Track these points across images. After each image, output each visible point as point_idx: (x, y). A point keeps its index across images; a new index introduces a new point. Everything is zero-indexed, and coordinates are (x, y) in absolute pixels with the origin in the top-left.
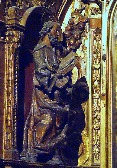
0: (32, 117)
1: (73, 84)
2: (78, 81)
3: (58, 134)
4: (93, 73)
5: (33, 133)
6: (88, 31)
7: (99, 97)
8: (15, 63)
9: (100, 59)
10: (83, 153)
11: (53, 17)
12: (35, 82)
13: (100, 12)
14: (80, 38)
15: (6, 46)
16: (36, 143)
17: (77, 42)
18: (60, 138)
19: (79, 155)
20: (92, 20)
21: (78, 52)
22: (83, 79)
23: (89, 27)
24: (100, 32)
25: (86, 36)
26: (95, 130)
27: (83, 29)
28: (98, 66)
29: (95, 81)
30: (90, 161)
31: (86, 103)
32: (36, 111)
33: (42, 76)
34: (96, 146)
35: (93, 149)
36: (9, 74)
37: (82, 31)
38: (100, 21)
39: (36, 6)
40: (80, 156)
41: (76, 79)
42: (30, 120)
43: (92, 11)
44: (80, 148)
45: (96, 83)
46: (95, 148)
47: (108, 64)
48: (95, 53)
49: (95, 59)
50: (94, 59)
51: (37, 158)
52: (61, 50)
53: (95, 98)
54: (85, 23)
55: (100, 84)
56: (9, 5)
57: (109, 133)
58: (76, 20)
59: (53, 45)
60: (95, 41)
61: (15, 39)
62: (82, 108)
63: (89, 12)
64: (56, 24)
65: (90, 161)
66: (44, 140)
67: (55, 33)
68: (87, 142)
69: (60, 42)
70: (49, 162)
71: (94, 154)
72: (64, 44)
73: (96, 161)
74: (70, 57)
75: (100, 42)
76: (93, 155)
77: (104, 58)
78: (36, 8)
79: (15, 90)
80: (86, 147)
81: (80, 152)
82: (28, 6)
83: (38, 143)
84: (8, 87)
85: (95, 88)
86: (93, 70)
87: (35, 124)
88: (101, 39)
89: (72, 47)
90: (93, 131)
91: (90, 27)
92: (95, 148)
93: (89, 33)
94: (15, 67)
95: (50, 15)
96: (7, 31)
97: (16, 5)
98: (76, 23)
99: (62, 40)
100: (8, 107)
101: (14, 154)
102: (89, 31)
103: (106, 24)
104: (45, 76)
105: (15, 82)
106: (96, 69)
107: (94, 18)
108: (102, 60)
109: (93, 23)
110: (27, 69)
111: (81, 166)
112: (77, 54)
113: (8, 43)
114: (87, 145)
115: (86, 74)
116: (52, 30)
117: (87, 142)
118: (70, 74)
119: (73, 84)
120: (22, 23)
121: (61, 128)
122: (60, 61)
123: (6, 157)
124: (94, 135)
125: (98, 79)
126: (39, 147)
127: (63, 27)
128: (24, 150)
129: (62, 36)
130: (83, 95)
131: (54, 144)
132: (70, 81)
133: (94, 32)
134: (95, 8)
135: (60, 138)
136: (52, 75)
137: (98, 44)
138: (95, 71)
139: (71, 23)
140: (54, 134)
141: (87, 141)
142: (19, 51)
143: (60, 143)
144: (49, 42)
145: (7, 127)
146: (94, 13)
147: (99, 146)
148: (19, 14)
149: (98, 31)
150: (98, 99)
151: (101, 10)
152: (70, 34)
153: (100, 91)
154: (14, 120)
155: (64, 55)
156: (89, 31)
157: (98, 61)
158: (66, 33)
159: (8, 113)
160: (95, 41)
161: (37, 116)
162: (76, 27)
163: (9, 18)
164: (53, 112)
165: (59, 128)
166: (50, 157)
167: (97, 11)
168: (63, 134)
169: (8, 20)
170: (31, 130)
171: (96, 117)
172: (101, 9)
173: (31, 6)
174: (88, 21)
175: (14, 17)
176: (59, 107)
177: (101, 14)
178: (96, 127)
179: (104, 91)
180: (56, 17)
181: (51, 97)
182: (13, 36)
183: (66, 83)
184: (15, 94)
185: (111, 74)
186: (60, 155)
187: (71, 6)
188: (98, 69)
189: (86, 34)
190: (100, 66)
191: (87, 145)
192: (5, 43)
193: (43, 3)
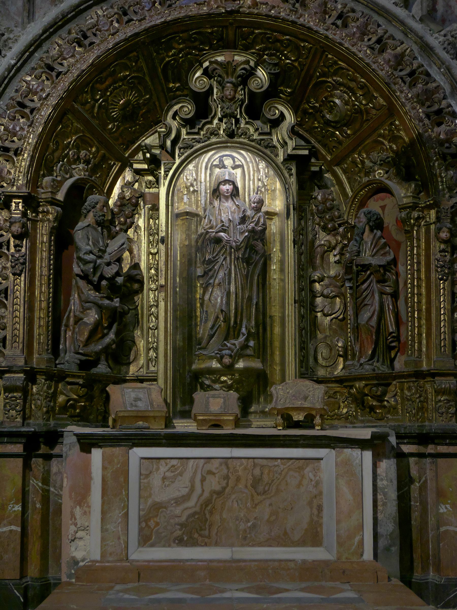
0: (72, 314)
1: (124, 272)
2: (130, 268)
4: (148, 259)
5: (72, 334)
6: (142, 208)
7: (157, 289)
8: (50, 246)
9: (158, 242)
10: (135, 359)
11: (98, 190)
12: (76, 270)
13: (157, 186)
14: (132, 216)
15: (39, 225)
16: (78, 347)
17: (128, 220)
18: (107, 340)
19: (131, 360)
20: (148, 195)
21: (130, 232)
22: (136, 266)
23: (144, 203)
24: (158, 210)
25: (140, 214)
26: (152, 329)
27: (137, 205)
28: (156, 250)
29: (151, 269)
30: (145, 368)
31: (140, 296)
32: (78, 306)
33: (86, 262)
34: (152, 350)
35: (148, 353)
36: (42, 259)
37: (134, 208)
38: (157, 196)
39: (77, 177)
40: (133, 361)
41: (128, 266)
42: (68, 317)
43: (146, 184)
44: (133, 353)
45: (153, 271)
46: (151, 353)
47: (167, 249)
48: (151, 235)
49: (151, 242)
50: (149, 242)
51: (79, 365)
52: (109, 231)
53: (152, 290)
54: (139, 198)
55: (158, 273)
56: (44, 176)
57: (169, 334)
58: (128, 194)
59: (99, 224)
60: (151, 220)
61: (50, 217)
62: (135, 303)
63: (144, 185)
64: (102, 198)
65: (145, 368)
66: (87, 342)
67: (102, 210)
68: (141, 344)
69: (107, 220)
70: (94, 371)
71: (150, 359)
72: (112, 222)
73: (152, 369)
74: (120, 240)
75: (157, 221)
76: (149, 360)
77: (163, 241)
78: (78, 179)
79: (49, 279)
80: (140, 351)
81: (132, 358)
82: (68, 176)
83: (79, 346)
84: (41, 275)
85: (151, 278)
86: (149, 256)
87: (76, 323)
88: (158, 218)
89: (122, 227)
90: (149, 331)
91: (145, 204)
92: (151, 353)
93: (144, 210)
94: (50, 250)
95: (95, 188)
96: (39, 206)
97: (52, 175)
98: (127, 198)
99: (110, 218)
100: (41, 301)
101: (49, 361)
102: (144, 207)
103: (165, 200)
104: (90, 262)
105: (50, 270)
106: (152, 254)
107: (150, 193)
108: (160, 244)
109: (148, 198)
110: (66, 253)
111: (133, 374)
112: (128, 235)
113: (42, 221)
114: (142, 349)
115: (140, 260)
116: (98, 206)
117: (141, 344)
118: (119, 260)
119: (124, 272)
120: (60, 196)
121: (110, 327)
122: (108, 244)
123: (37, 365)
124: (150, 336)
125: (155, 266)
126: (81, 351)
127: (111, 202)
128: (62, 355)
129: (110, 213)
130: (136, 286)
131: (100, 347)
132: (121, 268)
133: (150, 209)
134: (150, 181)
135: (107, 340)
136: (99, 261)
137: (155, 223)
138: (151, 256)
139: (121, 197)
140: (100, 335)
141: (141, 344)
142: (55, 231)
143: (108, 346)
144: (94, 220)
145: (40, 326)
146: (149, 186)
147: (156, 349)
148: (57, 186)
149: (155, 208)
150: (155, 291)
151: (158, 184)
152: (121, 211)
153: (157, 281)
154: (49, 317)
155: (112, 237)
156: (144, 207)
157: (155, 244)
158: (115, 210)
159: (40, 309)
160: (151, 220)
161: (77, 313)
162: (127, 202)
163: (43, 191)
164: (100, 307)
165: (106, 328)
166: (95, 363)
167: (154, 184)
168: (112, 336)
169: (43, 193)
170: (70, 330)
171: (152, 314)
172: (158, 181)
173: (71, 177)
174: (142, 195)
175: (50, 190)
176: (106, 302)
177: (158, 188)
178: (153, 326)
179: (162, 282)
180: (102, 189)
181: (97, 288)
182: (48, 212)
183: (115, 271)
184: (49, 284)
185: (171, 261)
186: (107, 361)
187: (121, 177)
188: (155, 254)
189: (140, 212)
190: (158, 251)
191: (142, 349)
192: (38, 221)
193: (87, 173)
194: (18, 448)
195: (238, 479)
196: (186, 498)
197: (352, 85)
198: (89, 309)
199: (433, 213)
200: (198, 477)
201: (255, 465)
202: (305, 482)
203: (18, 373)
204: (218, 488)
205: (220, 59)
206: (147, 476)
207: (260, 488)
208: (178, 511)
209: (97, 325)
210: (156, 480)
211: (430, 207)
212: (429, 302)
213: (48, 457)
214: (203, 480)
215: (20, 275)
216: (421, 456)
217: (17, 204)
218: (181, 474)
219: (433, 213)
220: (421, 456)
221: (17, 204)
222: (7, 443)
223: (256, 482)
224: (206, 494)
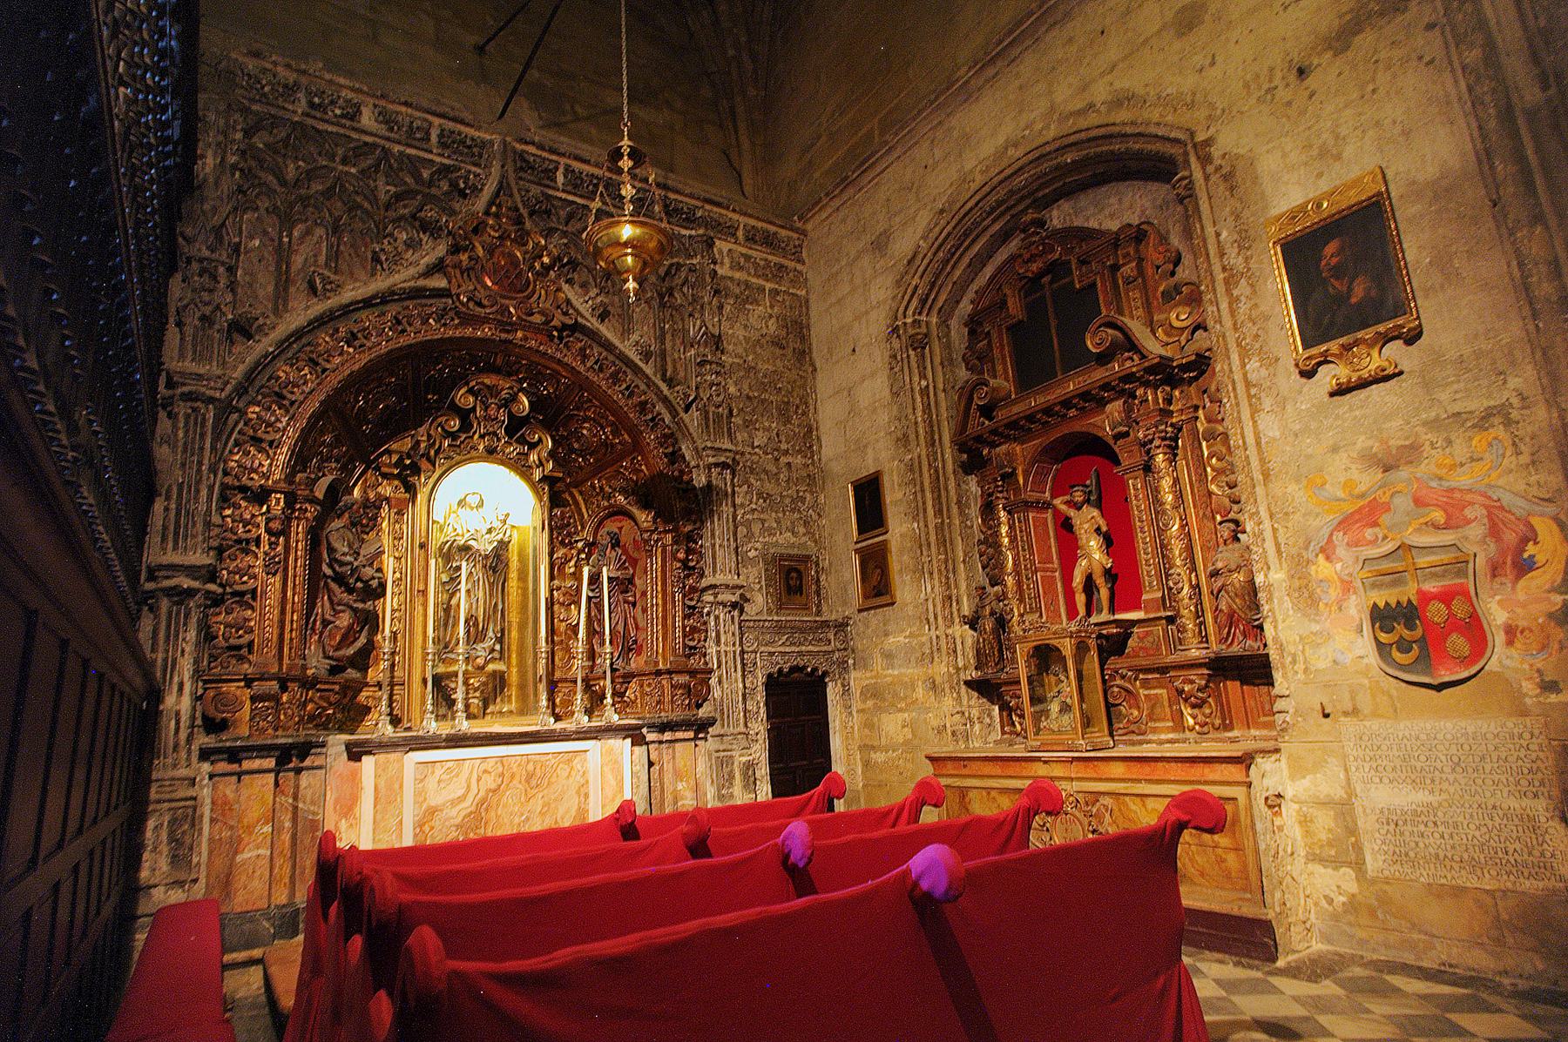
3: (356, 639)
194: (270, 763)
195: (513, 776)
196: (462, 799)
197: (602, 421)
198: (343, 611)
199: (669, 537)
200: (475, 776)
201: (528, 762)
202: (573, 773)
203: (271, 680)
204: (493, 786)
205: (487, 381)
206: (422, 781)
207: (534, 783)
208: (454, 812)
209: (350, 627)
210: (431, 783)
211: (666, 532)
212: (665, 610)
213: (298, 771)
214: (479, 780)
215: (274, 575)
216: (661, 742)
217: (278, 500)
218: (457, 775)
219: (669, 537)
220: (661, 742)
221: (278, 500)
222: (256, 757)
223: (530, 776)
224: (482, 793)
